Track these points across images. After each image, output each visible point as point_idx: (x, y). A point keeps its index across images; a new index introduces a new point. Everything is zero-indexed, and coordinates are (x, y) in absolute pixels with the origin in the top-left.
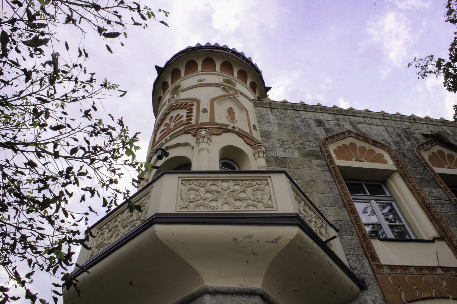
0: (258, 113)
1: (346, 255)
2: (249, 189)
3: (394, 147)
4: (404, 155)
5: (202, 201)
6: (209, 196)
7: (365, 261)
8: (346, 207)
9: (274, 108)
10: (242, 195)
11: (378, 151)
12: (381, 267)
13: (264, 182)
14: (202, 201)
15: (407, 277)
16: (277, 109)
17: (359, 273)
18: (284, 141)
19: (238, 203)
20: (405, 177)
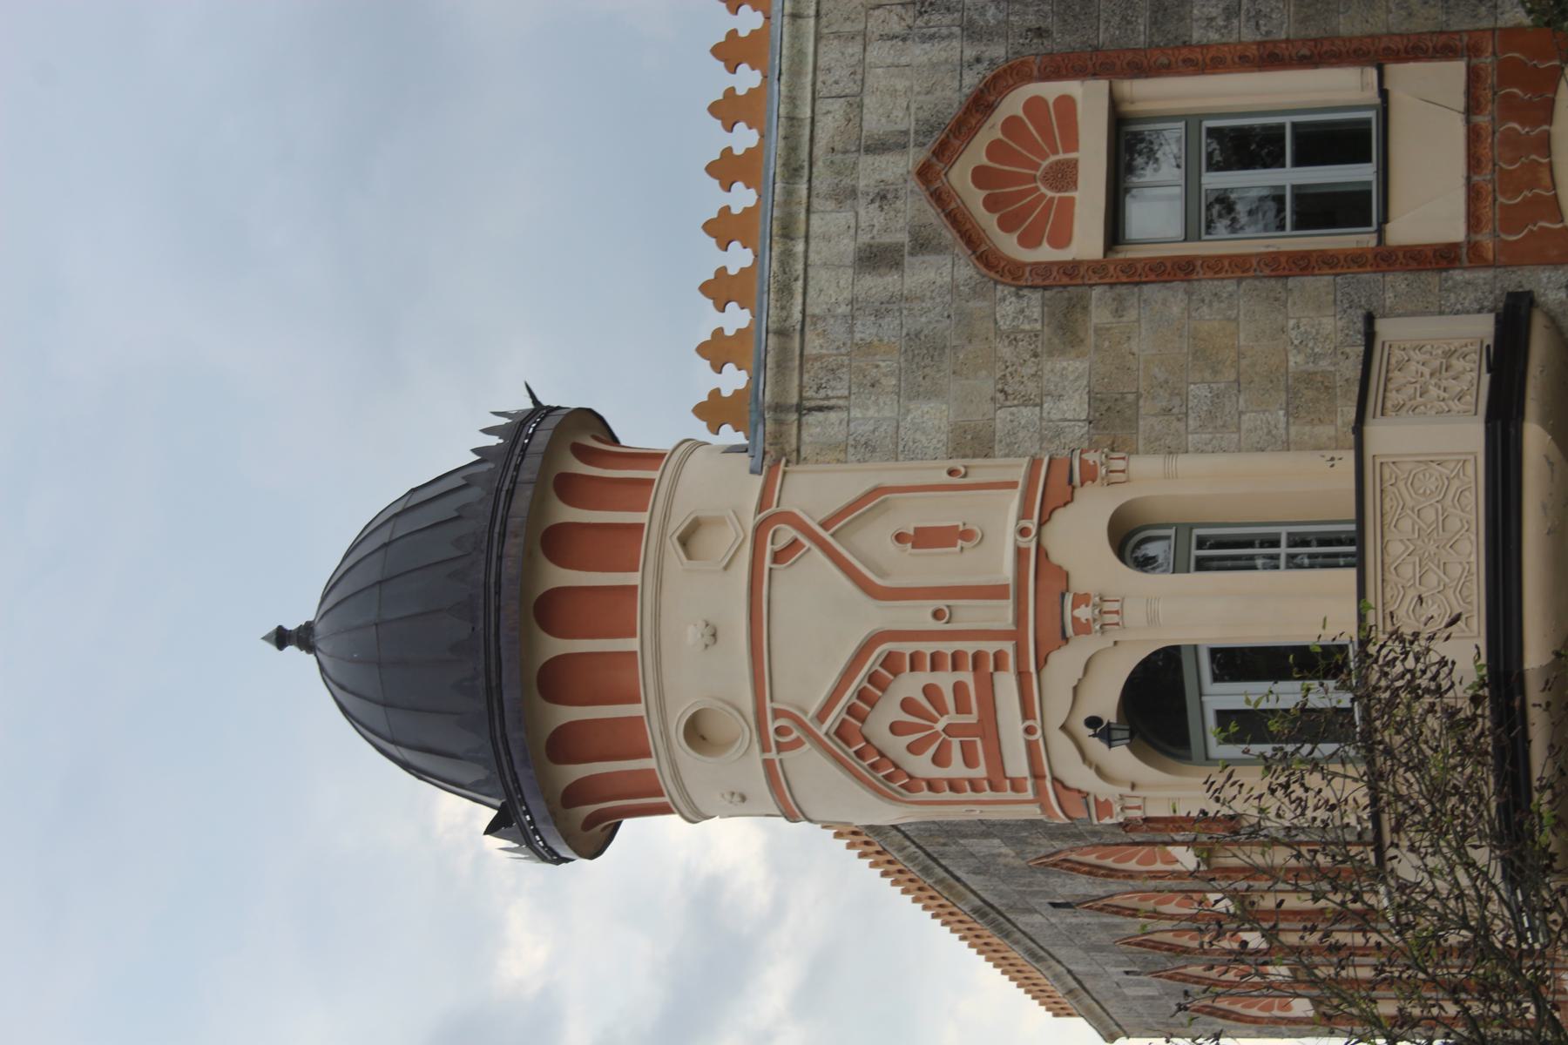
0: (842, 456)
1: (1441, 313)
2: (1410, 503)
3: (998, 51)
4: (1040, 32)
5: (1450, 592)
6: (1432, 579)
7: (1458, 275)
8: (1287, 277)
9: (801, 397)
10: (1430, 515)
11: (1013, 104)
12: (1474, 248)
13: (1387, 471)
14: (1450, 592)
15: (1501, 199)
16: (801, 387)
17: (1491, 298)
18: (1002, 391)
19: (1454, 524)
20: (1141, 70)
